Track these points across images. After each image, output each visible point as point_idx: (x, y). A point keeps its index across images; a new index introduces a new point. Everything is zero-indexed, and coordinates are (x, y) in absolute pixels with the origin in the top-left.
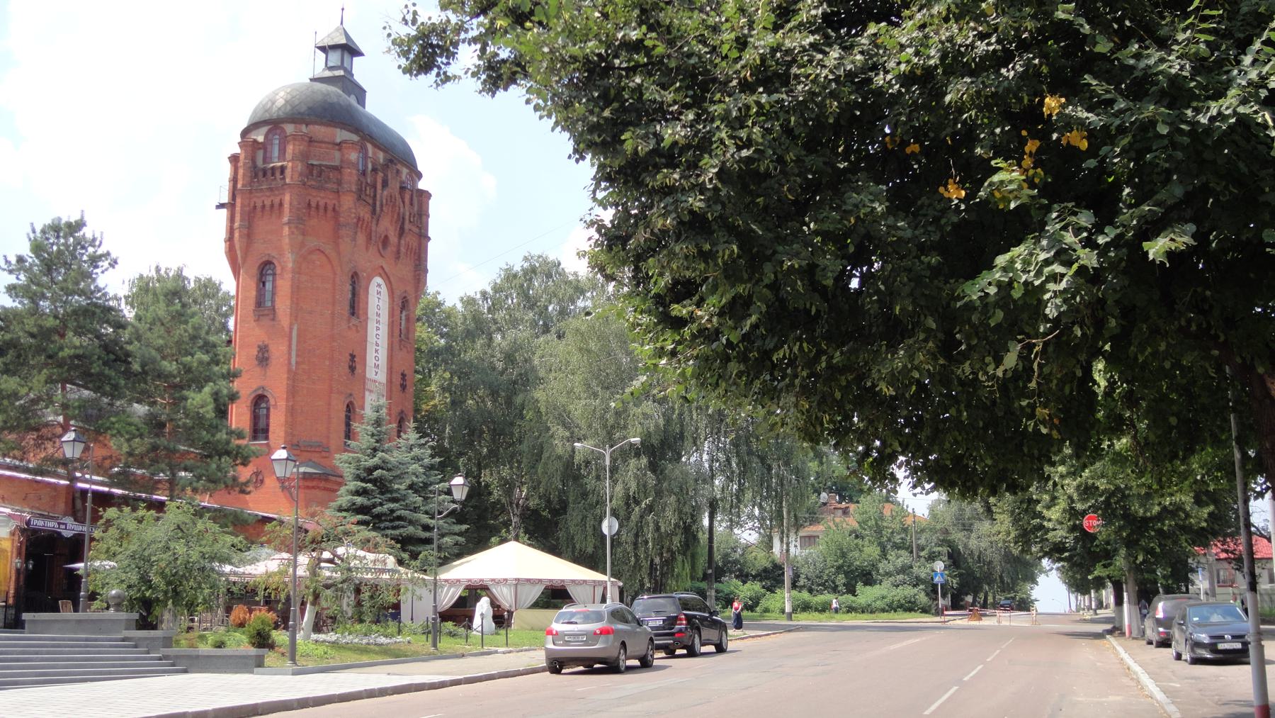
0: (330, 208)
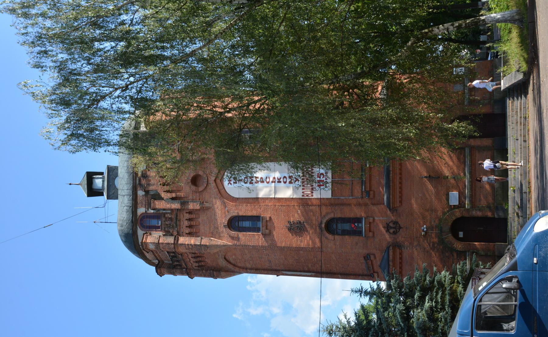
0: (193, 255)
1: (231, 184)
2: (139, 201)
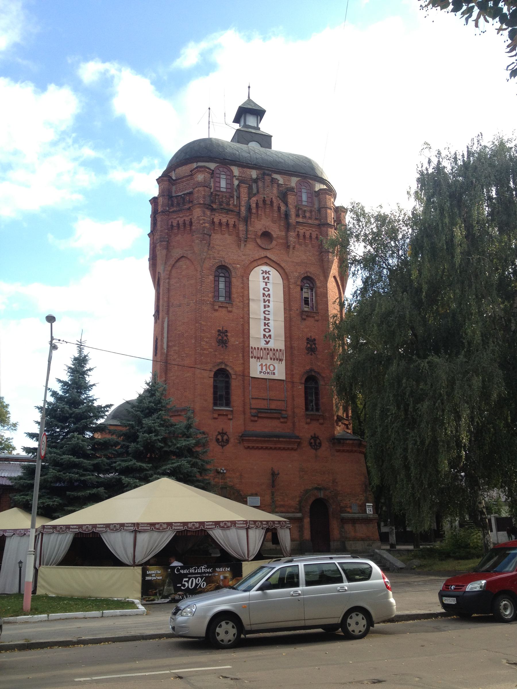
0: (187, 223)
1: (262, 273)
2: (245, 169)
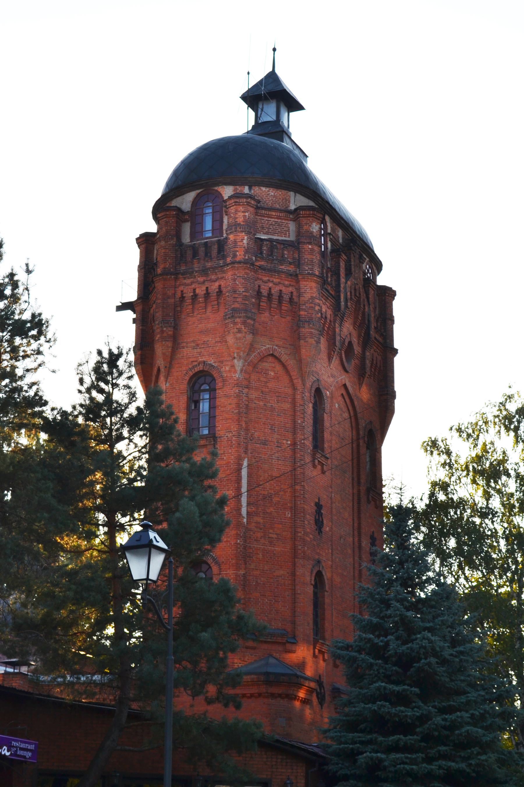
0: (286, 297)
